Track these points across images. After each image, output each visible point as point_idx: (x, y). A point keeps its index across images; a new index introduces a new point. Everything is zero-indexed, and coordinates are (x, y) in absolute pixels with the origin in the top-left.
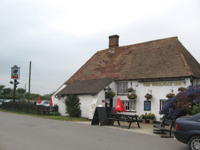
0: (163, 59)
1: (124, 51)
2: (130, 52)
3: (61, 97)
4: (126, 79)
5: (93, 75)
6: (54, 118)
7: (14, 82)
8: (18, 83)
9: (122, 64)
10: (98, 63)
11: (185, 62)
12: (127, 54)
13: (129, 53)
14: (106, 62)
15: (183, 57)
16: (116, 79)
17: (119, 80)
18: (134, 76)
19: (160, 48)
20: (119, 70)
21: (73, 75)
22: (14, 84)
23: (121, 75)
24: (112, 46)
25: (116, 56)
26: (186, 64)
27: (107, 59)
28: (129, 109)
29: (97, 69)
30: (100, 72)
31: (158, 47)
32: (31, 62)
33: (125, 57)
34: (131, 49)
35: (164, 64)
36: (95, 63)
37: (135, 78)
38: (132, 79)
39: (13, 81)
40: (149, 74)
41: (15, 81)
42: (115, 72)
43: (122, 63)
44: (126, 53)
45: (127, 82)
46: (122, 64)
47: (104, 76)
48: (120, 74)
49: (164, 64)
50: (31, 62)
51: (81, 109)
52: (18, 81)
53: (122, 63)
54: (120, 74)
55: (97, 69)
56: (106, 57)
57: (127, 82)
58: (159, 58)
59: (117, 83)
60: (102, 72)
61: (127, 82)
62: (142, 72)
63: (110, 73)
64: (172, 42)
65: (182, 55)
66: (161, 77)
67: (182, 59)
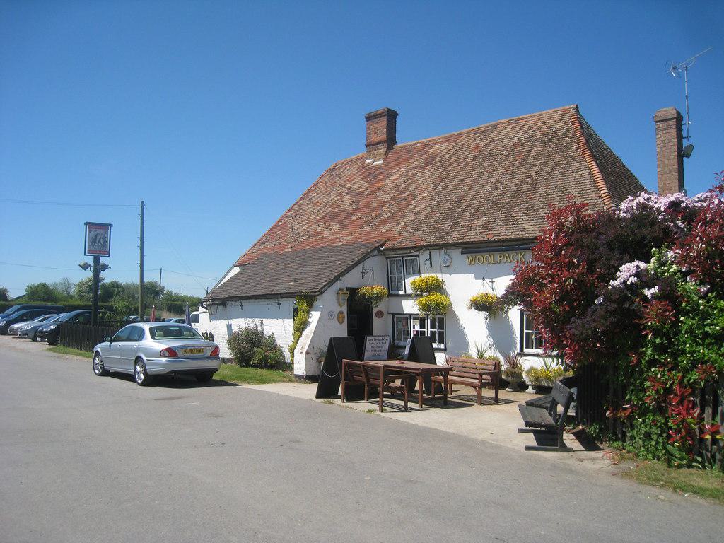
0: (530, 177)
1: (412, 158)
2: (430, 161)
3: (219, 304)
4: (413, 244)
5: (317, 233)
6: (35, 329)
7: (92, 264)
8: (105, 267)
9: (403, 200)
10: (333, 198)
11: (601, 184)
12: (420, 168)
13: (426, 164)
14: (358, 195)
15: (595, 170)
16: (382, 246)
17: (390, 250)
18: (438, 232)
19: (521, 144)
20: (395, 217)
21: (262, 239)
22: (92, 269)
23: (399, 234)
24: (374, 144)
25: (388, 173)
26: (604, 191)
27: (359, 184)
28: (441, 341)
29: (331, 218)
30: (336, 226)
31: (516, 140)
32: (143, 202)
33: (413, 175)
34: (431, 151)
35: (534, 194)
36: (323, 199)
37: (440, 241)
38: (430, 246)
39: (90, 260)
40: (485, 226)
41: (97, 260)
42: (384, 222)
43: (405, 196)
44: (418, 164)
45: (417, 253)
46: (403, 200)
47: (349, 238)
48: (395, 229)
49: (534, 194)
50: (143, 202)
51: (39, 283)
52: (103, 260)
53: (405, 196)
54: (395, 229)
55: (331, 218)
56: (359, 179)
57: (417, 253)
58: (518, 174)
59: (387, 258)
60: (343, 225)
61: (418, 255)
62: (465, 220)
63: (367, 229)
64: (562, 124)
65: (592, 165)
66: (523, 235)
67: (591, 175)
